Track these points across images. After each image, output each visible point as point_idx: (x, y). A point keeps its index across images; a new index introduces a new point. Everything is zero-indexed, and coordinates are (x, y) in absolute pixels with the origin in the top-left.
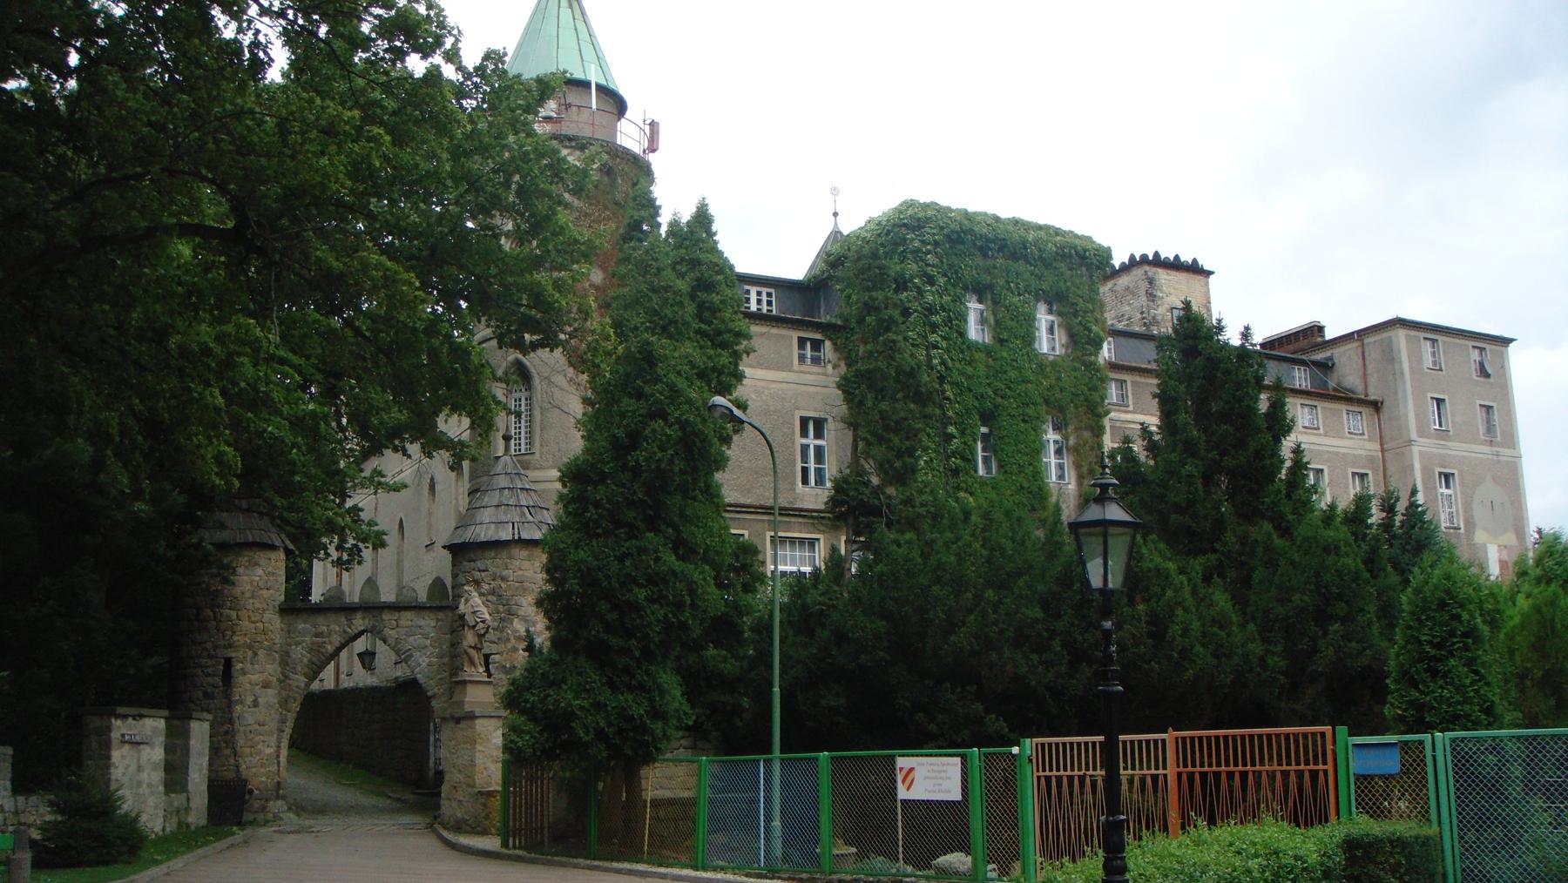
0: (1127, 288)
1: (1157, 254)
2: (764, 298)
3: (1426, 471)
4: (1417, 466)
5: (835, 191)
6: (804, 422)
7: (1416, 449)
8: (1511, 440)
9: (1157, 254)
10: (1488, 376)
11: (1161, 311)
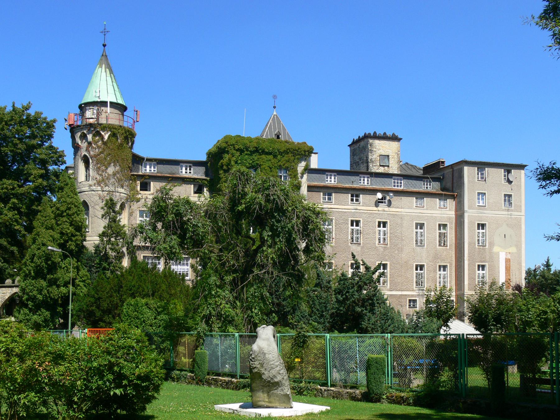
0: (363, 147)
1: (375, 133)
2: (188, 169)
3: (470, 223)
7: (466, 215)
9: (375, 133)
10: (512, 182)
11: (374, 157)
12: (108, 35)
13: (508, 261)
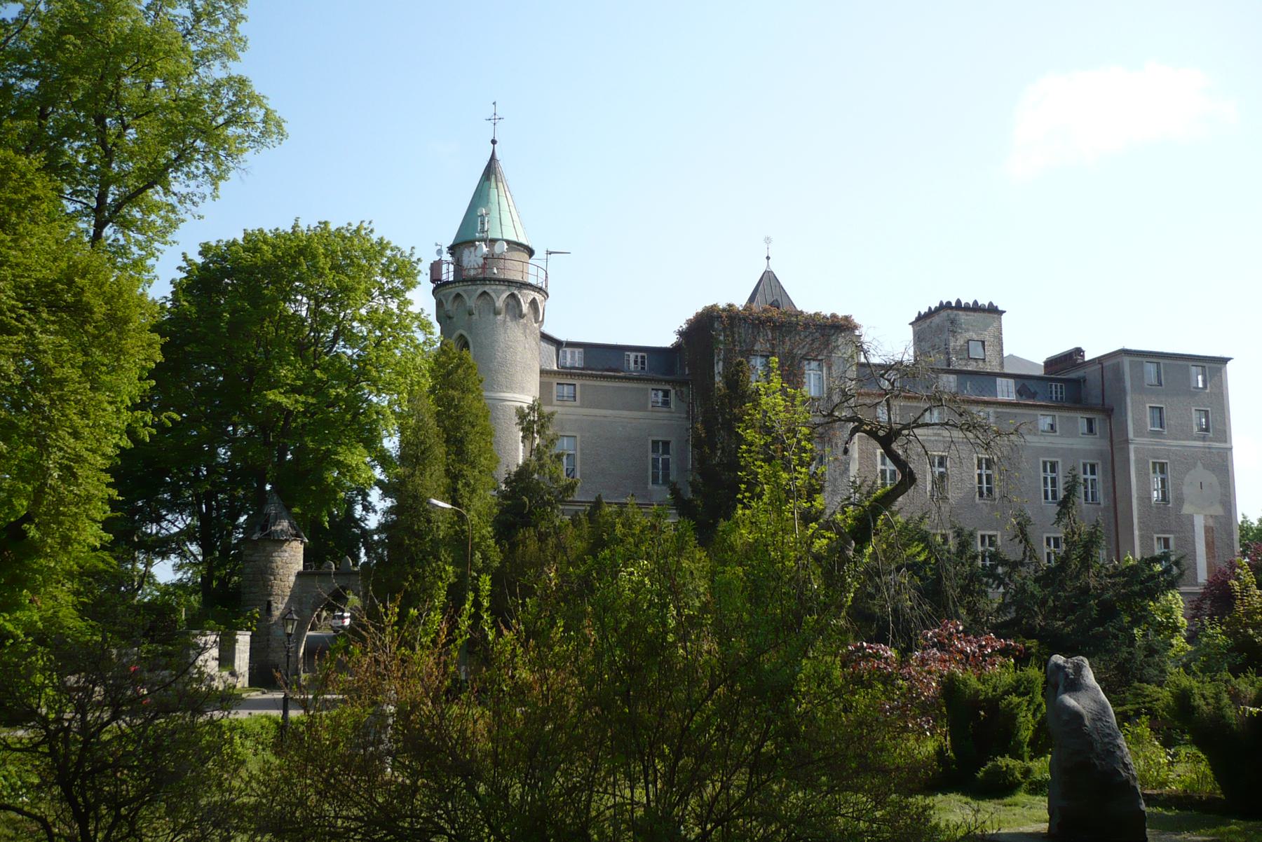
1: (959, 302)
3: (1141, 462)
4: (1132, 457)
5: (768, 240)
6: (655, 443)
7: (1132, 447)
8: (1223, 434)
9: (959, 302)
12: (499, 123)
13: (1208, 530)
